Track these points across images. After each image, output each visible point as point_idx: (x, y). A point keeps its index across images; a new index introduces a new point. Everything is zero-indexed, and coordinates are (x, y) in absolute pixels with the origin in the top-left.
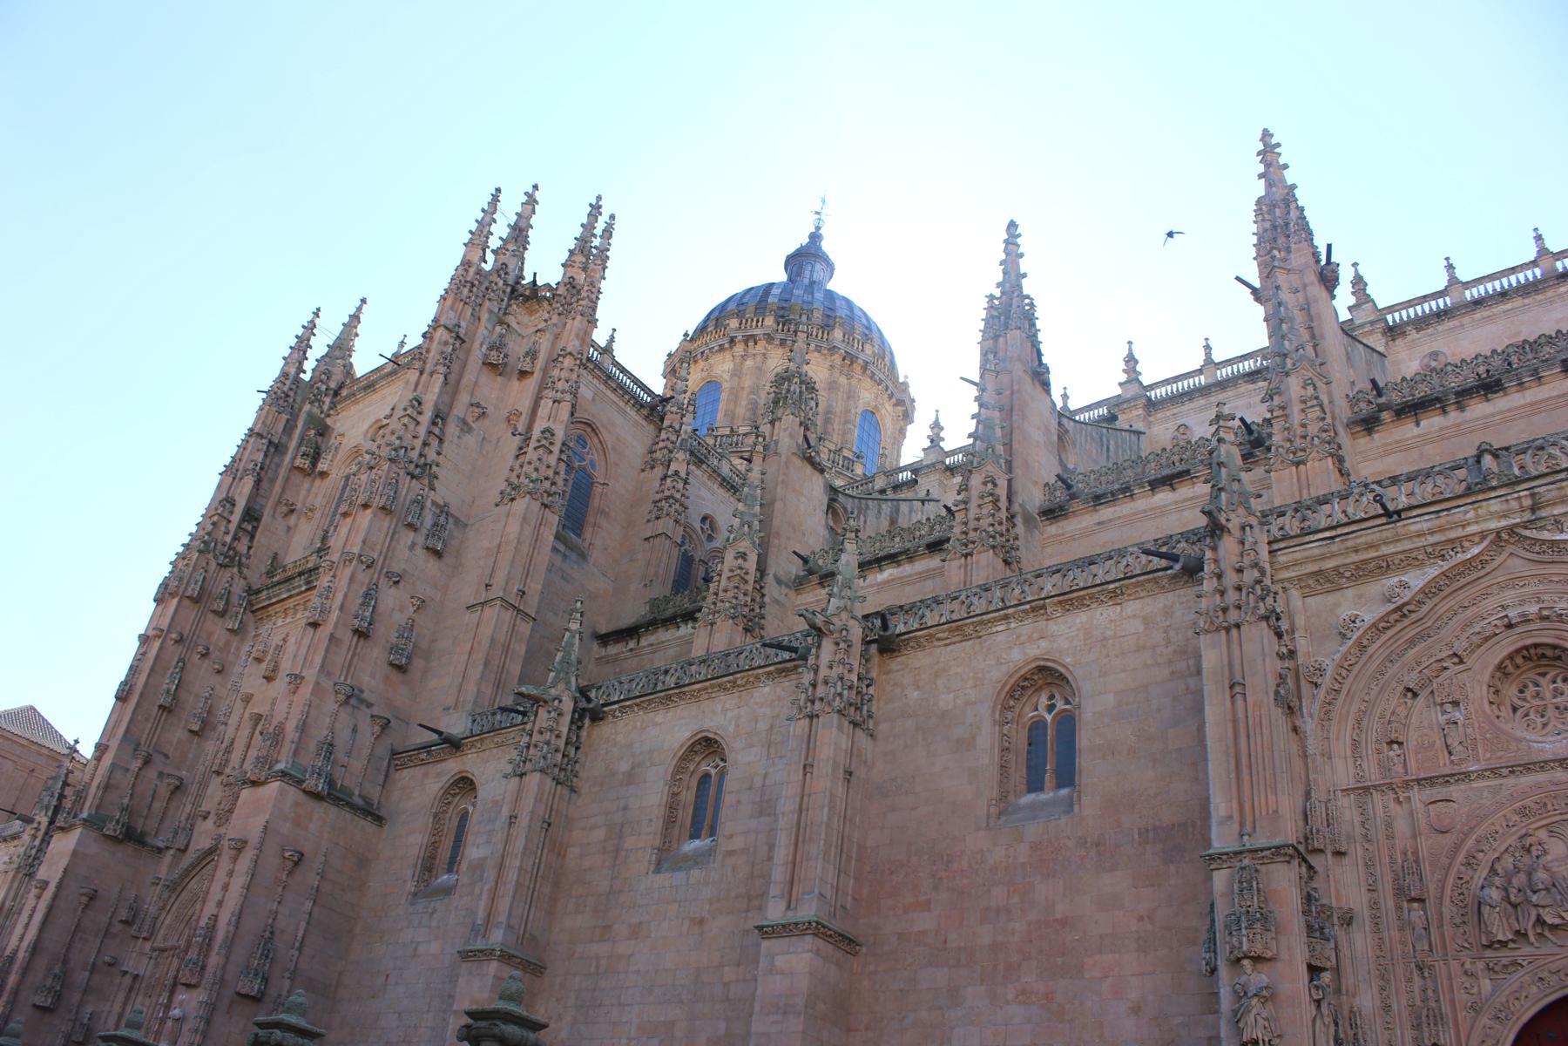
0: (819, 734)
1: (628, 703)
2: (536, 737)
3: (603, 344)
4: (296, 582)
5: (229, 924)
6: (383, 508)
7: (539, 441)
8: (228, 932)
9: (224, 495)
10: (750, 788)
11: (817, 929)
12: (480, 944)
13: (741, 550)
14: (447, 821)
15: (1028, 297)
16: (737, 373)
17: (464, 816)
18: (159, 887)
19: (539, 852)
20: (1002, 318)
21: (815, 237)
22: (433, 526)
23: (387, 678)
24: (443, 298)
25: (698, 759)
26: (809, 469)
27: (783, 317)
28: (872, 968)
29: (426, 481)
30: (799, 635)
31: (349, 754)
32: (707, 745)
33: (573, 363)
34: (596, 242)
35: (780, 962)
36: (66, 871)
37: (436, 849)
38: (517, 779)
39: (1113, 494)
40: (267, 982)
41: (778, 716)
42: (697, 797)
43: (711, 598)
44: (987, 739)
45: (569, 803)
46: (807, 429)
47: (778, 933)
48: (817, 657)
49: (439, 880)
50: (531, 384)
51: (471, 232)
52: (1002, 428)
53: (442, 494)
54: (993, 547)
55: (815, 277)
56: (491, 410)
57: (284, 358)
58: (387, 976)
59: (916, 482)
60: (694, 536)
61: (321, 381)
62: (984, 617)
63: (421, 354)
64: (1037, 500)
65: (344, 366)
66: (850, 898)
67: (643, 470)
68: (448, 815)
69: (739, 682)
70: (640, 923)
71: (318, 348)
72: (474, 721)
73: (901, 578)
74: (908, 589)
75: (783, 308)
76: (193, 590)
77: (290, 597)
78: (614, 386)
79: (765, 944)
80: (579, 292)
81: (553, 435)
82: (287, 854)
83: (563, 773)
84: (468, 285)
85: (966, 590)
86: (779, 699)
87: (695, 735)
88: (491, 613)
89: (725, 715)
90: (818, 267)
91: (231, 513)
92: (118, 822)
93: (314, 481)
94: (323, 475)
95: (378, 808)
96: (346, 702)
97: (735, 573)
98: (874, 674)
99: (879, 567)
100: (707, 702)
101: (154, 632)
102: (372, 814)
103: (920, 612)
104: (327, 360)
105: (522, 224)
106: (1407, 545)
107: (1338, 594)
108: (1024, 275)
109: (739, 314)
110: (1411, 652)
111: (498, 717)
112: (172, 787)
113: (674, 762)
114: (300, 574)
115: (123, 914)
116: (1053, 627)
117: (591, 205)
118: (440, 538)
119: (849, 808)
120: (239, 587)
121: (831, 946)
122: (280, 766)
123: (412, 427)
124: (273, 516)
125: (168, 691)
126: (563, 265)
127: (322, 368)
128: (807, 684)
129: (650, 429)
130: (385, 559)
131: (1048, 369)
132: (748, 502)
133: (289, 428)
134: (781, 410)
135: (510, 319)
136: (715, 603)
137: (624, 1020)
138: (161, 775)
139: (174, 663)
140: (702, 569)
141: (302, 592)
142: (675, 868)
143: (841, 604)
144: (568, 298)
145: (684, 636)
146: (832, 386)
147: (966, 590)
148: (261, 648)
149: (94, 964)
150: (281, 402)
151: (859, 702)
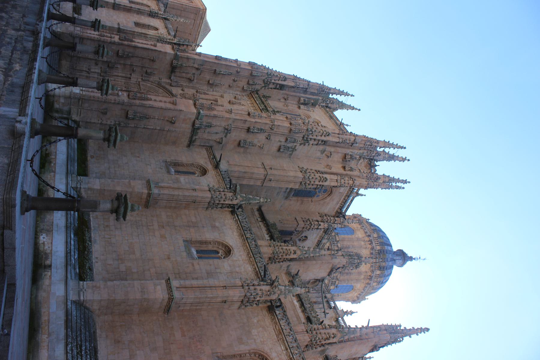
0: (236, 290)
1: (239, 222)
2: (223, 193)
3: (359, 192)
4: (263, 105)
5: (149, 104)
6: (291, 130)
7: (322, 177)
8: (147, 105)
9: (287, 77)
10: (216, 268)
11: (171, 299)
12: (152, 186)
13: (297, 252)
14: (191, 168)
15: (403, 339)
16: (358, 239)
17: (194, 173)
18: (159, 80)
19: (185, 200)
20: (393, 331)
21: (411, 259)
22: (288, 147)
23: (235, 140)
24: (365, 137)
25: (223, 249)
26: (328, 271)
27: (381, 252)
28: (160, 319)
29: (302, 142)
30: (270, 277)
31: (209, 133)
32: (228, 251)
33: (351, 184)
34: (394, 184)
35: (159, 287)
36: (160, 51)
37: (182, 166)
38: (208, 189)
40: (133, 119)
42: (210, 250)
43: (279, 244)
44: (243, 348)
45: (203, 208)
46: (342, 268)
47: (168, 285)
48: (263, 285)
49: (172, 169)
50: (342, 171)
51: (389, 141)
52: (354, 337)
53: (299, 148)
54: (311, 340)
55: (397, 261)
56: (330, 159)
57: (335, 88)
58: (139, 157)
59: (331, 308)
60: (300, 234)
61: (330, 101)
62: (286, 341)
63: (345, 133)
64: (331, 354)
65: (336, 108)
66: (183, 308)
67: (319, 213)
68: (194, 168)
69: (251, 259)
70: (166, 238)
71: (341, 98)
72: (225, 171)
73: (296, 309)
74: (292, 312)
75: (384, 252)
76: (255, 73)
77: (257, 104)
78: (346, 199)
79: (164, 281)
80: (375, 181)
81: (325, 181)
82: (174, 119)
83: (212, 204)
84: (371, 144)
85: (294, 333)
86: (247, 274)
87: (231, 247)
88: (262, 171)
89: (239, 256)
90: (401, 261)
91: (282, 81)
92: (177, 64)
93: (297, 105)
94: (299, 108)
95: (193, 145)
96: (225, 129)
97: (289, 251)
98: (260, 305)
99: (299, 301)
100: (243, 249)
101: (239, 64)
102: (191, 143)
103: (284, 318)
104: (338, 102)
105: (395, 158)
109: (379, 237)
111: (228, 179)
112: (190, 78)
113: (221, 241)
115: (149, 71)
117: (406, 180)
118: (284, 150)
119: (213, 303)
120: (258, 87)
121: (166, 304)
123: (320, 134)
124: (283, 94)
125: (221, 71)
126: (384, 174)
127: (334, 101)
128: (254, 283)
129: (333, 213)
130: (274, 133)
131: (378, 350)
132: (313, 252)
133: (313, 94)
134: (347, 258)
135: (362, 160)
136: (277, 246)
137: (134, 237)
138: (194, 74)
139: (230, 72)
140: (289, 239)
141: (259, 108)
142: (186, 246)
143: (283, 290)
144: (373, 178)
145: (264, 237)
146: (360, 273)
147: (294, 333)
148: (239, 98)
149: (132, 65)
150: (321, 90)
151: (250, 302)
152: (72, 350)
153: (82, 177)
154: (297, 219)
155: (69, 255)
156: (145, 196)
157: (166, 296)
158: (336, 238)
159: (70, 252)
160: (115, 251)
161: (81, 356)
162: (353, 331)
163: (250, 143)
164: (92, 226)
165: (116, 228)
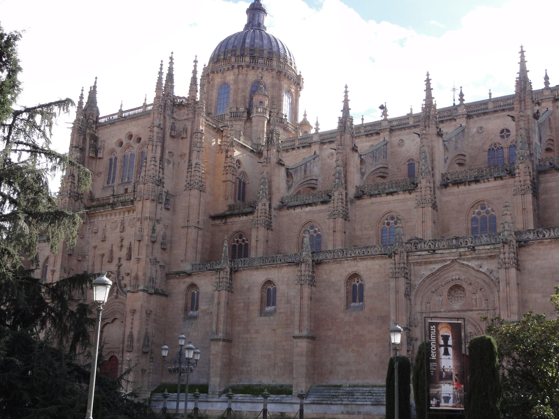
2: (221, 280)
11: (308, 337)
12: (216, 337)
16: (236, 82)
26: (280, 166)
27: (252, 54)
32: (269, 282)
35: (299, 344)
39: (375, 195)
42: (268, 294)
44: (343, 291)
49: (189, 313)
50: (187, 142)
67: (218, 153)
72: (193, 266)
79: (295, 340)
82: (148, 312)
91: (74, 180)
94: (100, 158)
102: (164, 294)
106: (436, 259)
107: (421, 267)
108: (350, 109)
110: (434, 283)
114: (109, 204)
116: (358, 264)
122: (141, 287)
123: (155, 168)
135: (175, 115)
146: (273, 85)
154: (224, 180)
155: (274, 401)
156: (224, 343)
157: (305, 340)
158: (234, 112)
159: (272, 400)
161: (338, 395)
162: (339, 174)
163: (163, 239)
164: (248, 383)
165: (249, 366)
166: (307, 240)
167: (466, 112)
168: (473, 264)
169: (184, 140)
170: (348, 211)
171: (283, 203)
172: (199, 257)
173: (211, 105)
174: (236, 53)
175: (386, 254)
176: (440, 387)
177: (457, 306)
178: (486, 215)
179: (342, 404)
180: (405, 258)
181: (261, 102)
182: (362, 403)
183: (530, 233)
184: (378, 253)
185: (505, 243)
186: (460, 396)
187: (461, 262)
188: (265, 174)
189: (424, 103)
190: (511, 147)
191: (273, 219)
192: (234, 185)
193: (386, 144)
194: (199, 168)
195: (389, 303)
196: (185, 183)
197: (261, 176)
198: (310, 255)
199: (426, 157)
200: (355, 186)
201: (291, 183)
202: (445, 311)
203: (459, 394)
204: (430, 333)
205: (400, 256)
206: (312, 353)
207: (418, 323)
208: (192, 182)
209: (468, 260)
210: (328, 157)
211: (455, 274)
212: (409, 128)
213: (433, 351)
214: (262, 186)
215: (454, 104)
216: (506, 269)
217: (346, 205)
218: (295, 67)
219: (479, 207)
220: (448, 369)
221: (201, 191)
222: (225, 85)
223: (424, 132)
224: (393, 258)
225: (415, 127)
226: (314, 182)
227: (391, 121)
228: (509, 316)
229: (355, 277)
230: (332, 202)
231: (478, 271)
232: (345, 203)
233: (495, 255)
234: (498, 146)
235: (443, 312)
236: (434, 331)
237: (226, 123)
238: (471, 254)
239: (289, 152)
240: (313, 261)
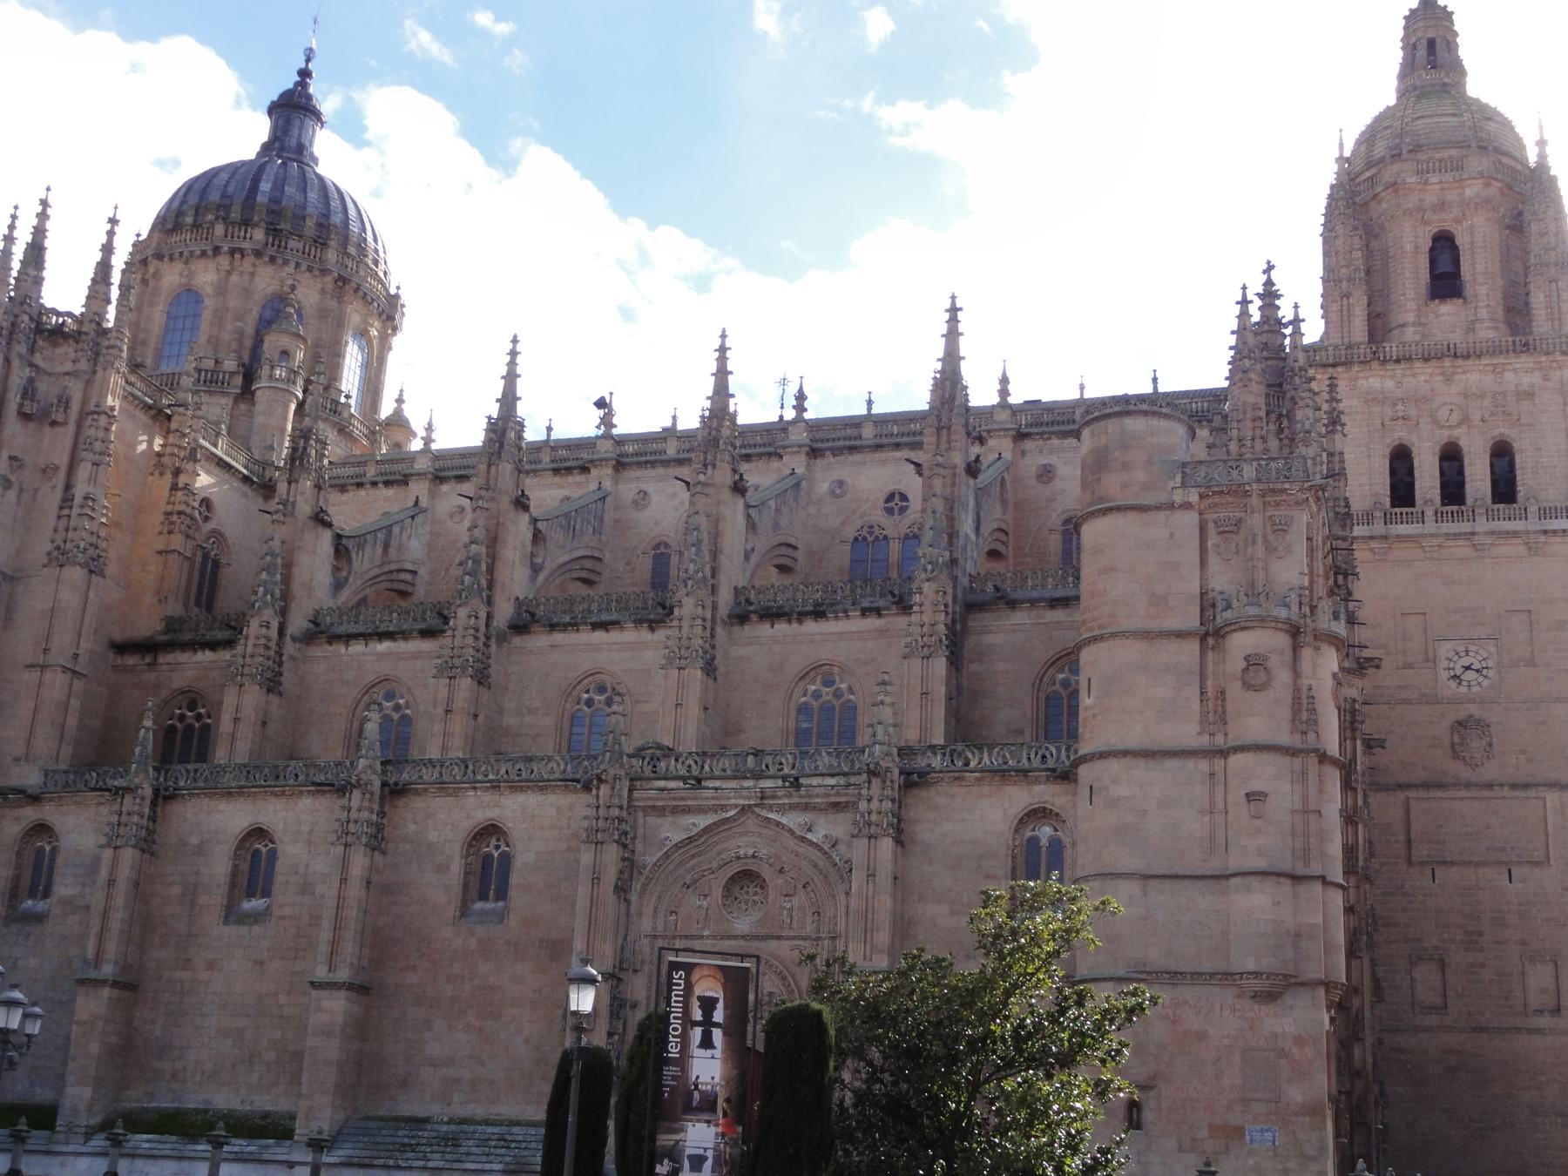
2: (124, 819)
7: (82, 507)
10: (296, 873)
11: (350, 987)
12: (93, 974)
13: (265, 618)
16: (221, 290)
21: (305, 74)
26: (320, 529)
27: (272, 223)
32: (259, 833)
35: (325, 1004)
41: (316, 823)
42: (251, 866)
44: (457, 867)
49: (24, 905)
67: (152, 474)
72: (46, 775)
79: (315, 993)
135: (38, 359)
146: (323, 313)
152: (407, 1159)
153: (59, 1122)
154: (161, 548)
155: (240, 1156)
156: (116, 992)
157: (343, 993)
158: (206, 371)
160: (233, 1066)
161: (417, 1145)
166: (372, 728)
167: (808, 441)
168: (792, 820)
169: (59, 430)
170: (491, 661)
171: (317, 624)
172: (67, 751)
173: (144, 343)
174: (228, 214)
175: (578, 781)
176: (682, 1130)
177: (743, 924)
178: (835, 702)
179: (425, 1168)
180: (625, 794)
181: (285, 353)
182: (479, 1166)
183: (935, 754)
184: (557, 776)
185: (873, 773)
186: (730, 1155)
187: (764, 813)
188: (276, 544)
189: (708, 404)
190: (907, 537)
191: (287, 666)
192: (186, 565)
193: (604, 498)
194: (93, 509)
195: (573, 906)
196: (49, 547)
197: (265, 547)
198: (379, 768)
199: (699, 542)
200: (513, 597)
201: (344, 574)
202: (714, 937)
203: (728, 1149)
204: (670, 991)
205: (613, 788)
206: (360, 1030)
207: (643, 962)
208: (69, 546)
209: (782, 809)
210: (451, 517)
211: (745, 844)
212: (666, 463)
213: (674, 1036)
214: (264, 575)
215: (781, 417)
216: (870, 838)
217: (487, 645)
218: (385, 273)
219: (819, 679)
220: (707, 1084)
221: (91, 572)
222: (189, 296)
223: (701, 477)
224: (594, 792)
225: (680, 462)
226: (407, 577)
227: (621, 441)
228: (868, 958)
229: (491, 835)
230: (449, 633)
231: (803, 839)
232: (483, 639)
233: (847, 802)
234: (877, 533)
235: (708, 937)
236: (679, 985)
237: (181, 395)
238: (790, 796)
239: (347, 491)
240: (384, 784)
